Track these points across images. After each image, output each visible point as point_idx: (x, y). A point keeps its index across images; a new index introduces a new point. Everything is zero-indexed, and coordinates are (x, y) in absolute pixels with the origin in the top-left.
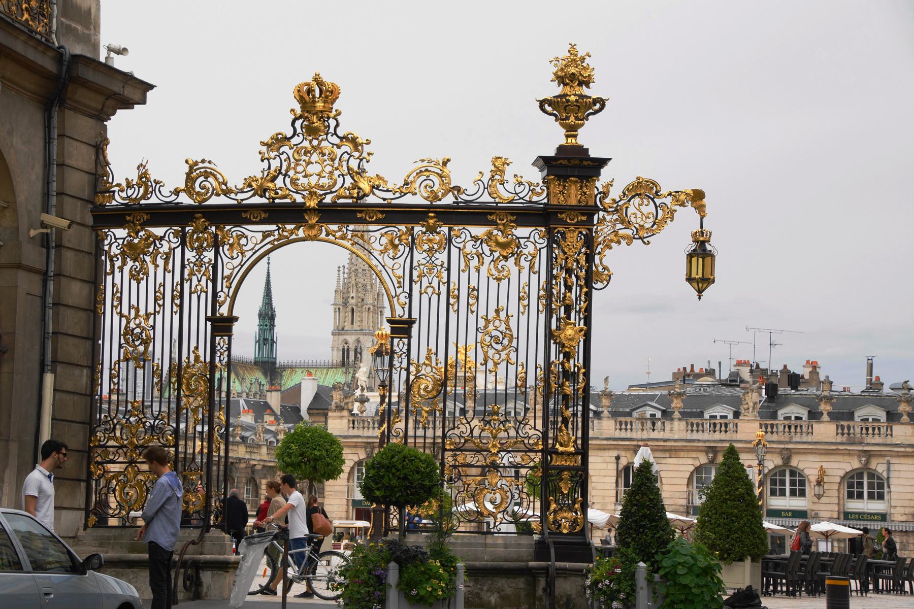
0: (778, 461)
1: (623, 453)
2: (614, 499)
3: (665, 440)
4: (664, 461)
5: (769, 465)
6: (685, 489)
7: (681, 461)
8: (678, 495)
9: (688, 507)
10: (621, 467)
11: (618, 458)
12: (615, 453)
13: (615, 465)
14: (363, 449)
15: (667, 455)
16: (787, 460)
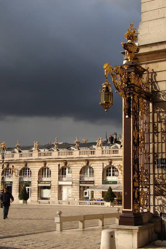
0: (108, 164)
1: (60, 163)
3: (72, 158)
4: (73, 165)
5: (105, 165)
6: (79, 175)
7: (78, 165)
8: (77, 177)
11: (59, 165)
12: (58, 163)
15: (74, 163)
16: (111, 163)
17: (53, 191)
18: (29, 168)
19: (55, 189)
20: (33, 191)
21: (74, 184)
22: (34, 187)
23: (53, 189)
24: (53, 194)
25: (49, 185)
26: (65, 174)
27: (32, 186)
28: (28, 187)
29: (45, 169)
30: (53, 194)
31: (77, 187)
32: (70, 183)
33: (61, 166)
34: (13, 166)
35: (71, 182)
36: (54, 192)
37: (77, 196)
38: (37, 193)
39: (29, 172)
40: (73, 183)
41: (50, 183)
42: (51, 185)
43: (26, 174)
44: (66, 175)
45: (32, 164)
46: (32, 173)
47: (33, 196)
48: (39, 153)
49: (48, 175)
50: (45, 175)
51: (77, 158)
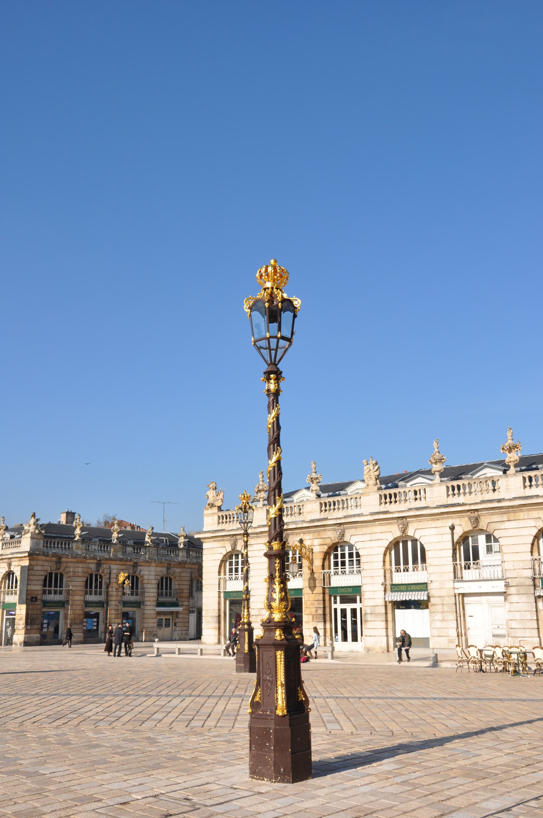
1: (456, 521)
2: (452, 575)
3: (499, 501)
4: (503, 526)
6: (529, 557)
7: (521, 524)
8: (521, 565)
9: (534, 579)
10: (456, 538)
11: (452, 528)
13: (450, 536)
14: (229, 542)
15: (505, 518)
17: (439, 616)
18: (352, 542)
19: (446, 609)
20: (369, 618)
21: (512, 590)
22: (372, 603)
23: (439, 608)
24: (438, 624)
25: (421, 596)
26: (476, 557)
27: (366, 602)
28: (353, 606)
29: (405, 543)
30: (438, 624)
31: (524, 598)
32: (500, 587)
33: (458, 532)
34: (301, 541)
35: (502, 583)
36: (443, 620)
37: (528, 633)
38: (383, 624)
39: (351, 555)
40: (507, 586)
41: (427, 590)
42: (429, 597)
43: (343, 564)
44: (478, 558)
45: (359, 531)
46: (362, 559)
47: (371, 632)
48: (380, 496)
49: (415, 561)
50: (406, 562)
51: (515, 499)
